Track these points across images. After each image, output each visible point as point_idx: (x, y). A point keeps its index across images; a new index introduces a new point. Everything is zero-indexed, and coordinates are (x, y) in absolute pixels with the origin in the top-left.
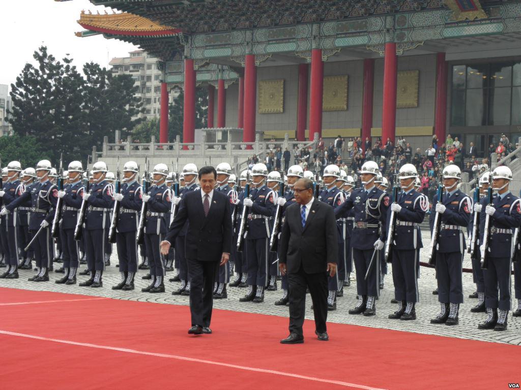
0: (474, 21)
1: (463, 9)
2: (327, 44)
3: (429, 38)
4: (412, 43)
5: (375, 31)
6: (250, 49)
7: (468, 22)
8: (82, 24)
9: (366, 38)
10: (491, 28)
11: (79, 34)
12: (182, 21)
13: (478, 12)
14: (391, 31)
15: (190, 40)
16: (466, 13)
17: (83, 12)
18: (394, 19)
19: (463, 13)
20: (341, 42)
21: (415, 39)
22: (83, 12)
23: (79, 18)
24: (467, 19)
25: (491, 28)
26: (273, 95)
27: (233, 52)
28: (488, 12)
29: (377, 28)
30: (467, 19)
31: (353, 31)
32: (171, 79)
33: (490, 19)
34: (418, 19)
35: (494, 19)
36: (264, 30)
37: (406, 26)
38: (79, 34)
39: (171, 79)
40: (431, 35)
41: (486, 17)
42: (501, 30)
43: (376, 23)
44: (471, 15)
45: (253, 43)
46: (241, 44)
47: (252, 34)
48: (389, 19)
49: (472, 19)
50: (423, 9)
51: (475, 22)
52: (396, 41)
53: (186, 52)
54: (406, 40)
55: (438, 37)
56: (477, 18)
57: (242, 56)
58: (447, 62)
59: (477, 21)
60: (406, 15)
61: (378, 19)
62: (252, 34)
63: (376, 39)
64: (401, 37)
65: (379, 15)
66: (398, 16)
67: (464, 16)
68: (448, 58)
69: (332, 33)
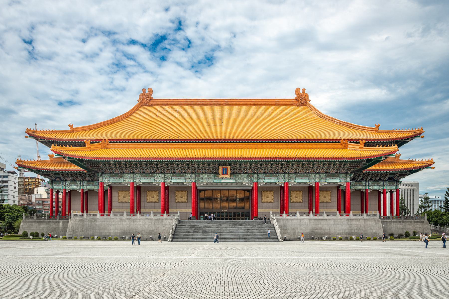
1: (223, 174)
7: (223, 178)
10: (231, 181)
27: (124, 181)
29: (189, 177)
32: (55, 187)
34: (204, 176)
36: (139, 174)
39: (55, 187)
44: (225, 176)
45: (134, 178)
51: (226, 178)
53: (101, 180)
55: (212, 182)
57: (129, 183)
64: (199, 181)
65: (189, 173)
67: (221, 176)
69: (170, 177)
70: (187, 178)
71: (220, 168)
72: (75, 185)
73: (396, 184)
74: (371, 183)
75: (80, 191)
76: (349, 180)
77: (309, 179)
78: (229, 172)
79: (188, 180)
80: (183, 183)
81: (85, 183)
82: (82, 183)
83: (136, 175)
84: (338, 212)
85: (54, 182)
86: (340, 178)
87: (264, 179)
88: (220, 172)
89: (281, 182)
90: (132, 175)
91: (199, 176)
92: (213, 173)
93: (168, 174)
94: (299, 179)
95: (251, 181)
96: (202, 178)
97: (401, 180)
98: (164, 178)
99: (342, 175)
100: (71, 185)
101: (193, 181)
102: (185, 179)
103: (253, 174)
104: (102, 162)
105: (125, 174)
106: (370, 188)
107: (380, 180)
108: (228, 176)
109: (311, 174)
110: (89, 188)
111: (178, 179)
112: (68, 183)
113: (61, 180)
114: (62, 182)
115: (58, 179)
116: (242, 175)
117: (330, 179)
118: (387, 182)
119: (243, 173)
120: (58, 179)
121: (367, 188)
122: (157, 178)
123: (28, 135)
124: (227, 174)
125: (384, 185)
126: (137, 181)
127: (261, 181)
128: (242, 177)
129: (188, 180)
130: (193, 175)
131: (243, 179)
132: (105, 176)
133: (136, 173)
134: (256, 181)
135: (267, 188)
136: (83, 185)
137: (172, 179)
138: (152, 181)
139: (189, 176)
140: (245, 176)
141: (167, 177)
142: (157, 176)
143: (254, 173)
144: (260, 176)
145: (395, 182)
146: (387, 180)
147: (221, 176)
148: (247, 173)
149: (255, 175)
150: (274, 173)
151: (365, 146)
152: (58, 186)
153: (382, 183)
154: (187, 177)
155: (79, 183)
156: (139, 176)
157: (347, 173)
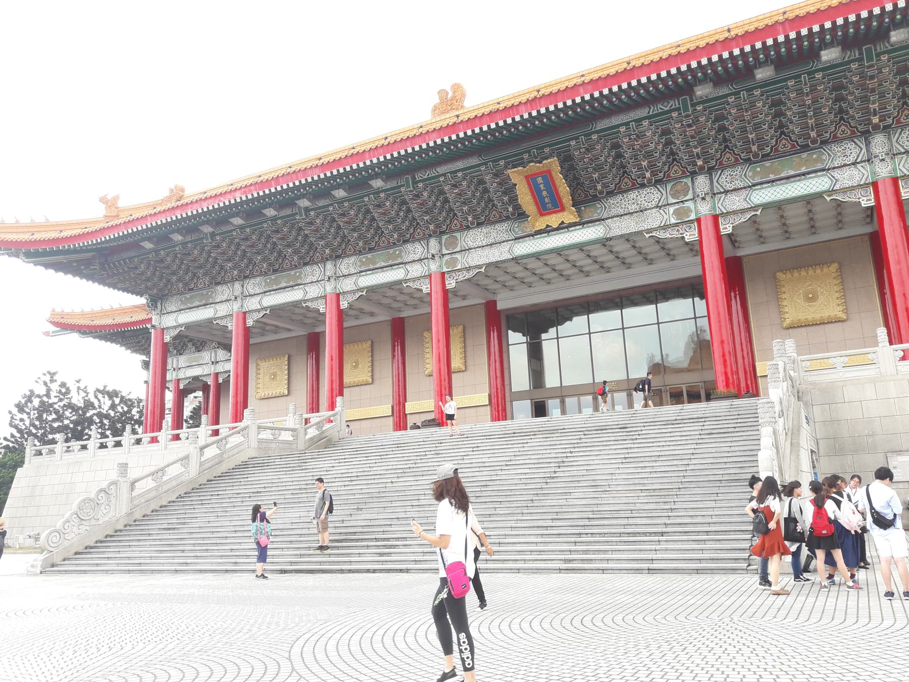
0: (558, 229)
1: (543, 211)
2: (347, 285)
4: (468, 269)
5: (414, 261)
6: (239, 304)
7: (548, 231)
8: (51, 322)
9: (402, 271)
11: (47, 334)
12: (148, 279)
13: (565, 213)
14: (437, 258)
15: (159, 305)
16: (547, 218)
17: (54, 310)
18: (440, 243)
19: (542, 219)
20: (368, 280)
21: (472, 264)
22: (54, 310)
23: (48, 316)
24: (548, 226)
26: (275, 375)
28: (579, 212)
29: (417, 257)
30: (548, 226)
31: (383, 264)
33: (582, 224)
34: (475, 237)
35: (588, 222)
36: (258, 279)
37: (458, 249)
38: (47, 334)
41: (578, 220)
42: (602, 235)
43: (415, 250)
44: (554, 220)
46: (227, 301)
47: (243, 286)
48: (433, 242)
49: (555, 226)
50: (479, 225)
52: (445, 270)
54: (459, 267)
56: (563, 222)
58: (499, 311)
59: (563, 228)
60: (457, 235)
62: (243, 286)
63: (416, 270)
66: (444, 237)
68: (500, 306)
69: (353, 271)
78: (564, 189)
88: (525, 199)
89: (848, 183)
90: (237, 285)
91: (453, 242)
101: (434, 267)
103: (688, 181)
105: (219, 288)
108: (569, 216)
116: (632, 195)
119: (643, 186)
127: (735, 202)
128: (633, 208)
132: (171, 306)
134: (704, 209)
140: (649, 196)
141: (346, 272)
142: (312, 272)
143: (693, 174)
144: (725, 179)
147: (541, 224)
149: (702, 181)
150: (805, 148)
156: (260, 284)
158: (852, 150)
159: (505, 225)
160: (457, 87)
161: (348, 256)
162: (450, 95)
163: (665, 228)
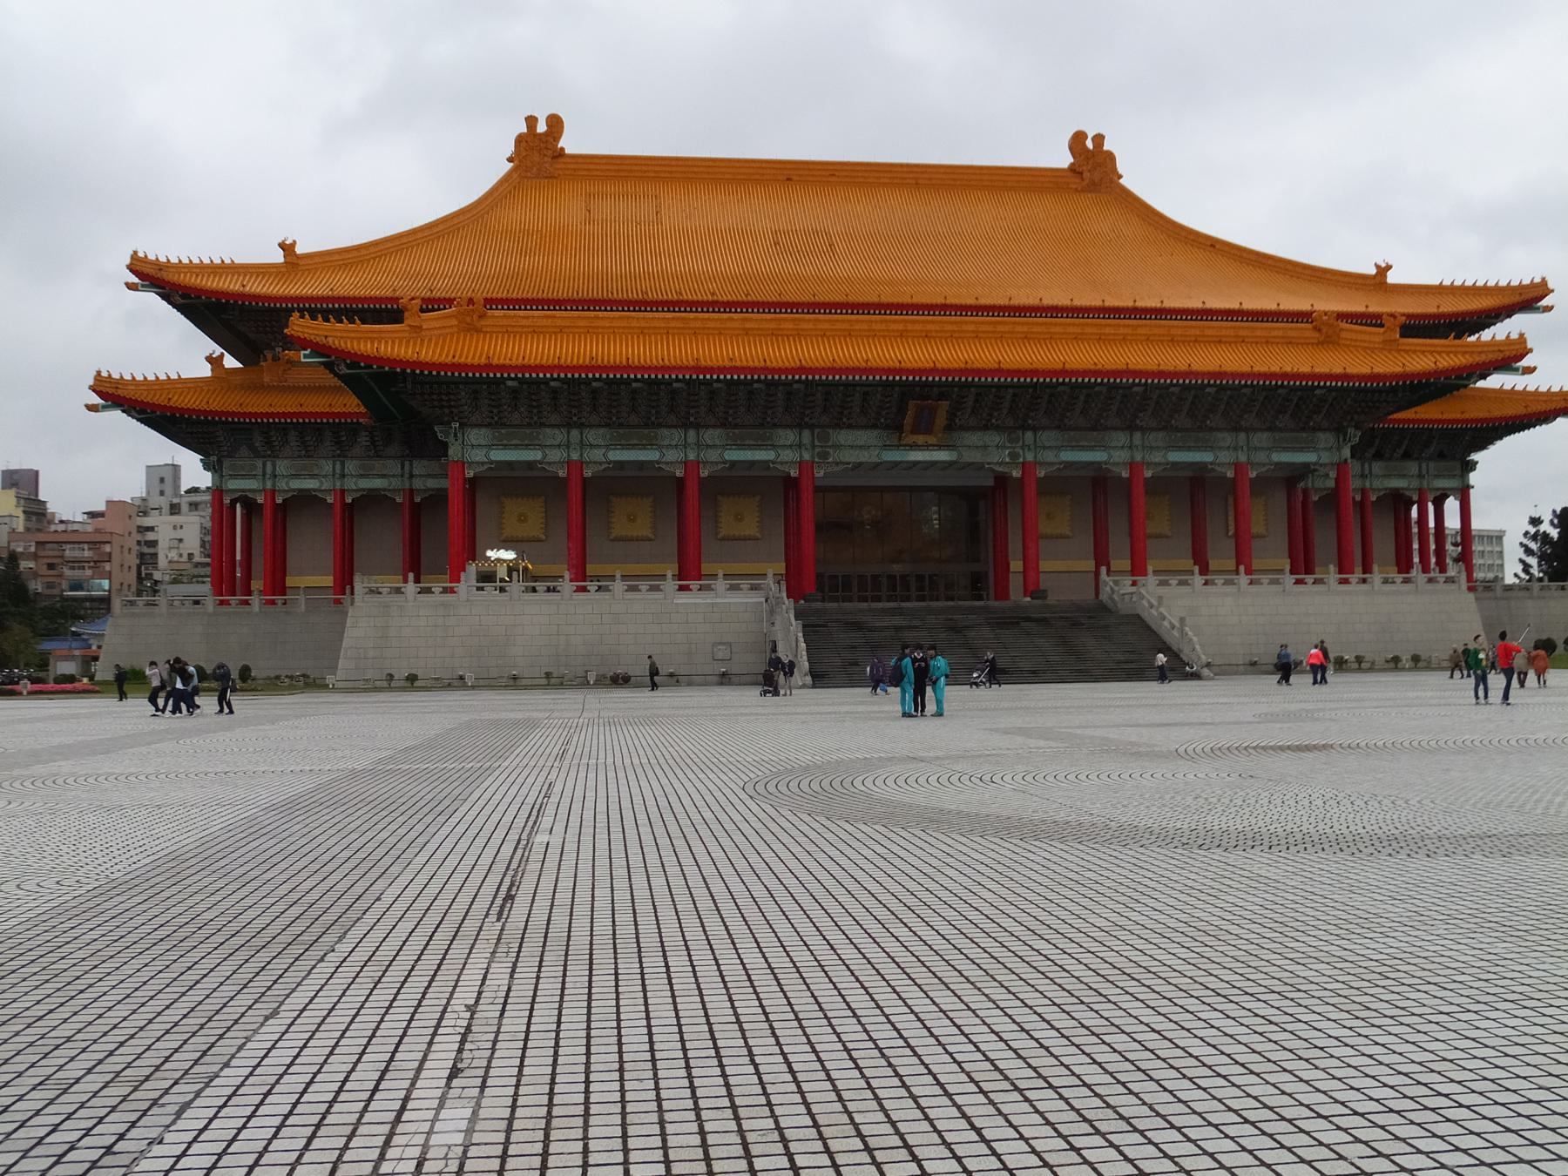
3: (863, 460)
7: (914, 447)
10: (943, 456)
11: (92, 408)
17: (99, 373)
22: (99, 373)
25: (943, 456)
27: (545, 456)
32: (233, 484)
33: (940, 447)
34: (844, 437)
38: (92, 408)
39: (233, 484)
40: (864, 457)
44: (920, 439)
45: (582, 445)
50: (850, 427)
51: (927, 447)
53: (454, 452)
55: (875, 459)
61: (789, 431)
64: (824, 455)
70: (785, 447)
71: (912, 403)
72: (313, 476)
73: (1458, 472)
74: (1377, 467)
75: (330, 500)
76: (1347, 452)
77: (1212, 448)
79: (782, 452)
80: (766, 462)
81: (351, 466)
82: (338, 466)
83: (592, 436)
84: (1196, 569)
85: (226, 463)
86: (1315, 450)
87: (1059, 448)
92: (874, 427)
93: (711, 431)
94: (1180, 449)
95: (1013, 455)
96: (837, 447)
97: (1475, 457)
98: (698, 445)
99: (1321, 435)
100: (296, 476)
102: (774, 447)
104: (467, 381)
106: (1377, 484)
107: (1407, 456)
108: (932, 440)
109: (1219, 435)
110: (366, 484)
111: (750, 447)
112: (282, 466)
113: (257, 455)
114: (259, 463)
115: (244, 451)
117: (1285, 449)
118: (1432, 464)
119: (985, 428)
120: (244, 451)
121: (1368, 485)
122: (669, 446)
123: (136, 280)
124: (928, 431)
125: (1421, 476)
126: (597, 454)
129: (782, 452)
130: (806, 433)
131: (985, 447)
133: (591, 426)
134: (1030, 457)
135: (1061, 484)
136: (343, 476)
137: (725, 447)
138: (533, 455)
139: (789, 436)
143: (1024, 428)
145: (1458, 464)
146: (1430, 459)
148: (997, 428)
149: (1029, 435)
151: (1402, 336)
152: (243, 476)
153: (1413, 467)
154: (781, 442)
155: (327, 466)
157: (1339, 430)
158: (1121, 438)
159: (876, 433)
160: (555, 123)
161: (714, 427)
162: (542, 128)
163: (1000, 464)
